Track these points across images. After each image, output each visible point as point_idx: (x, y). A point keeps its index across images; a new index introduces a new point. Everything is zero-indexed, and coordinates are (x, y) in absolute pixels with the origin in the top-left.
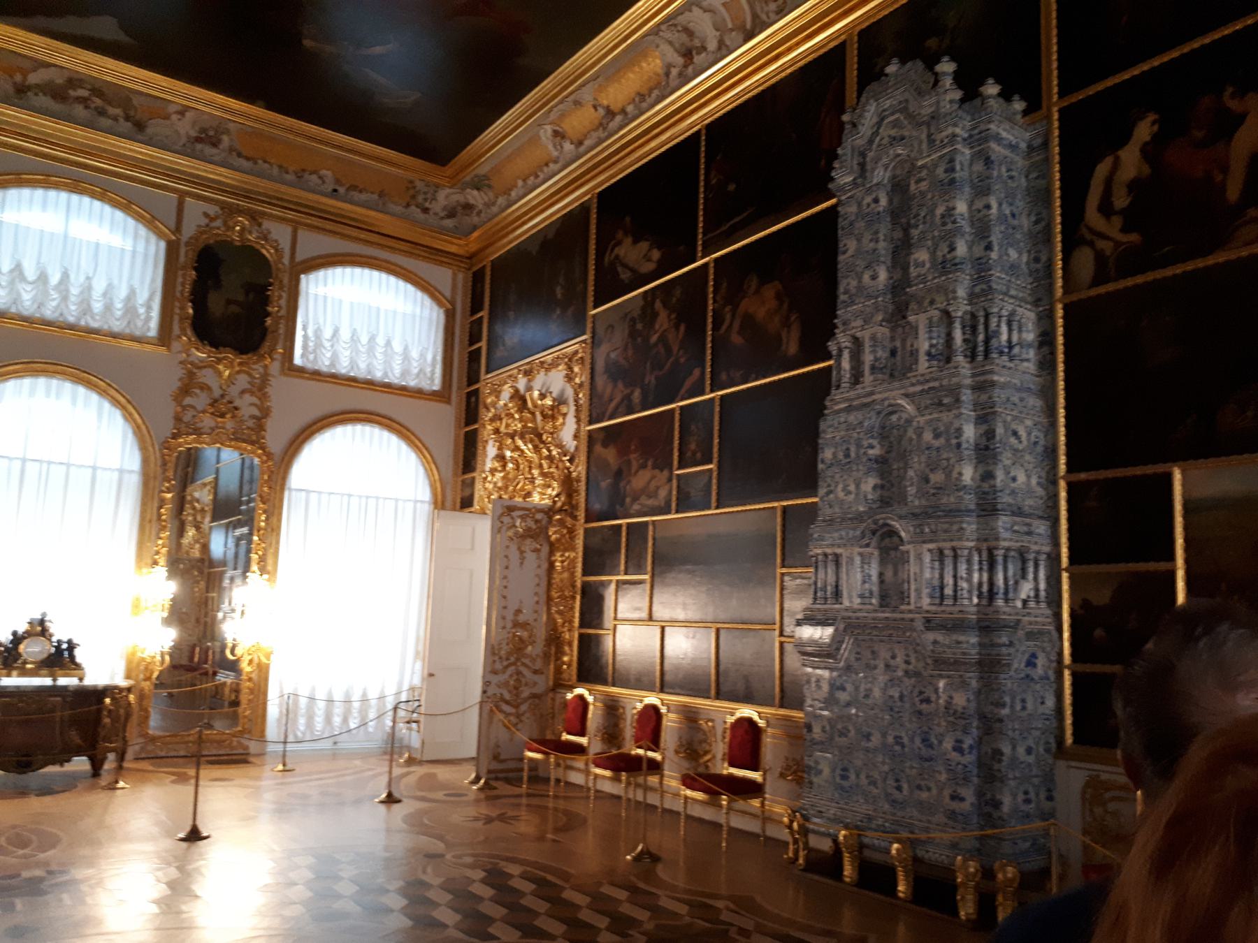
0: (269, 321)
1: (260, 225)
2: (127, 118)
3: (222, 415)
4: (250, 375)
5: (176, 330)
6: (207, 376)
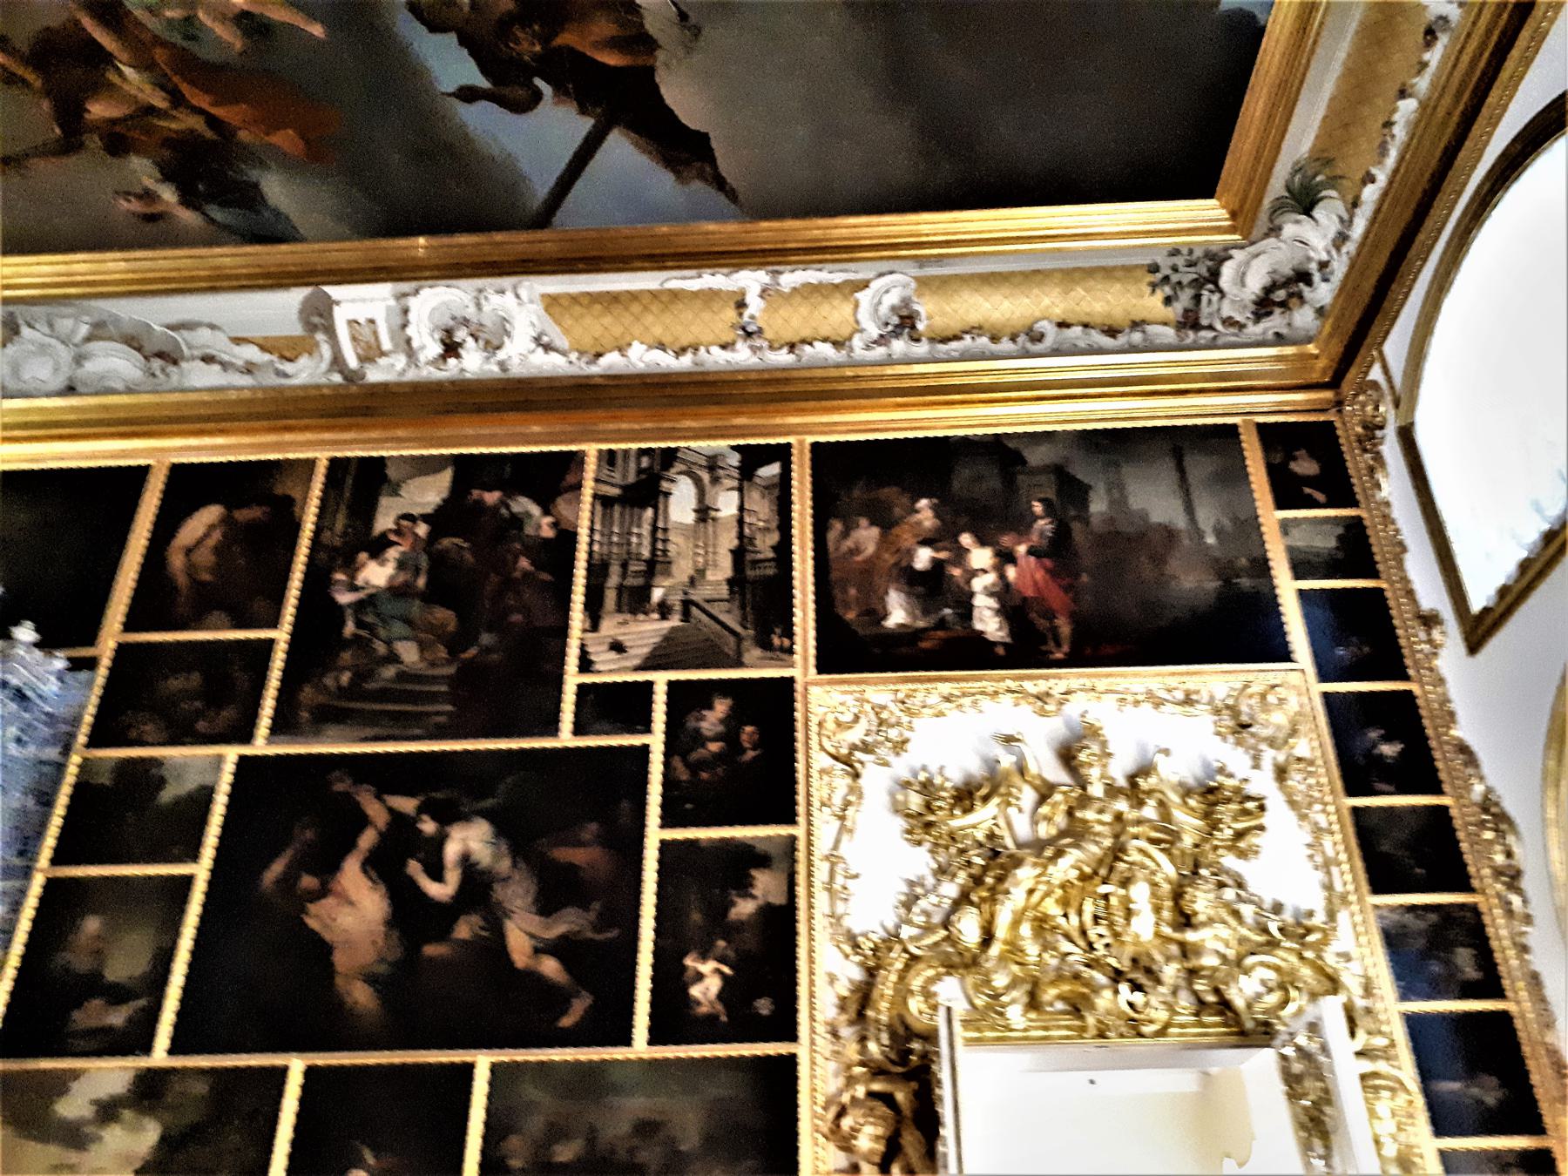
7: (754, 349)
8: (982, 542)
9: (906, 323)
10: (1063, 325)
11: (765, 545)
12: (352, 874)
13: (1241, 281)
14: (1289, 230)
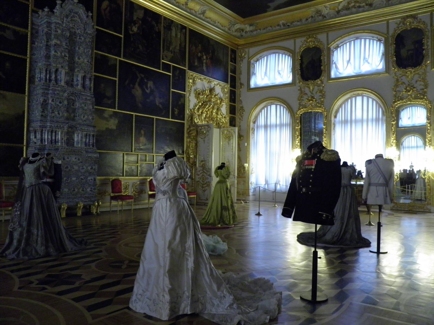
0: (424, 52)
1: (417, 18)
2: (367, 5)
3: (409, 91)
4: (418, 74)
5: (391, 66)
6: (404, 79)
7: (186, 7)
8: (205, 55)
9: (203, 13)
10: (218, 22)
11: (183, 44)
12: (137, 86)
13: (236, 27)
14: (246, 26)
